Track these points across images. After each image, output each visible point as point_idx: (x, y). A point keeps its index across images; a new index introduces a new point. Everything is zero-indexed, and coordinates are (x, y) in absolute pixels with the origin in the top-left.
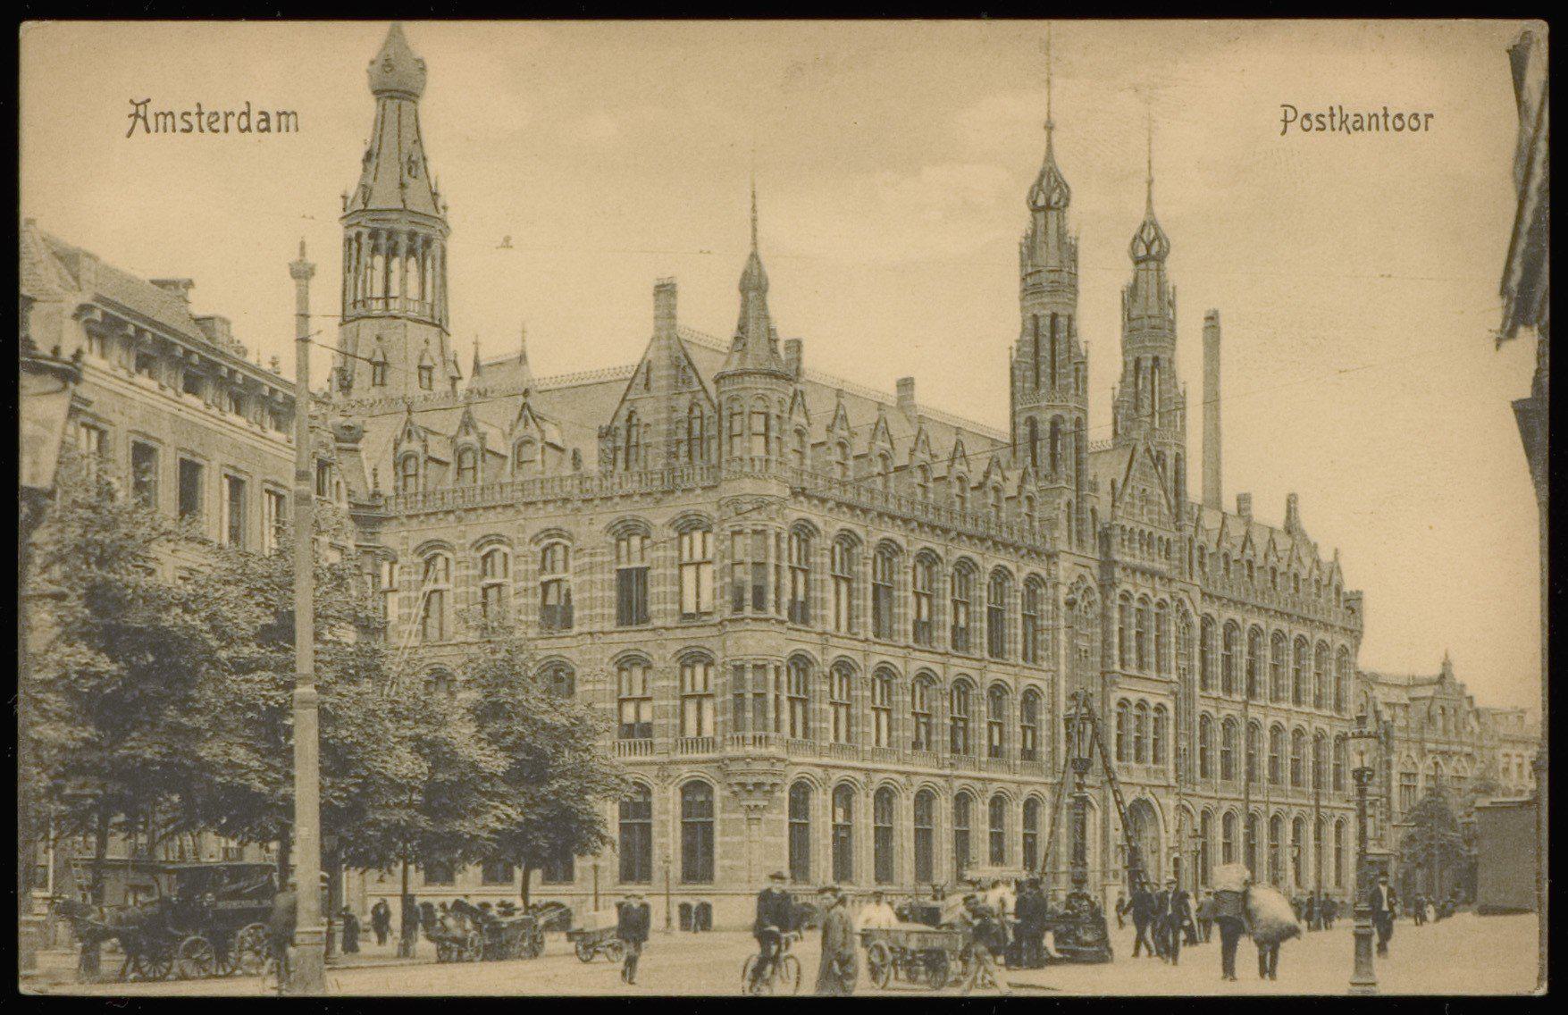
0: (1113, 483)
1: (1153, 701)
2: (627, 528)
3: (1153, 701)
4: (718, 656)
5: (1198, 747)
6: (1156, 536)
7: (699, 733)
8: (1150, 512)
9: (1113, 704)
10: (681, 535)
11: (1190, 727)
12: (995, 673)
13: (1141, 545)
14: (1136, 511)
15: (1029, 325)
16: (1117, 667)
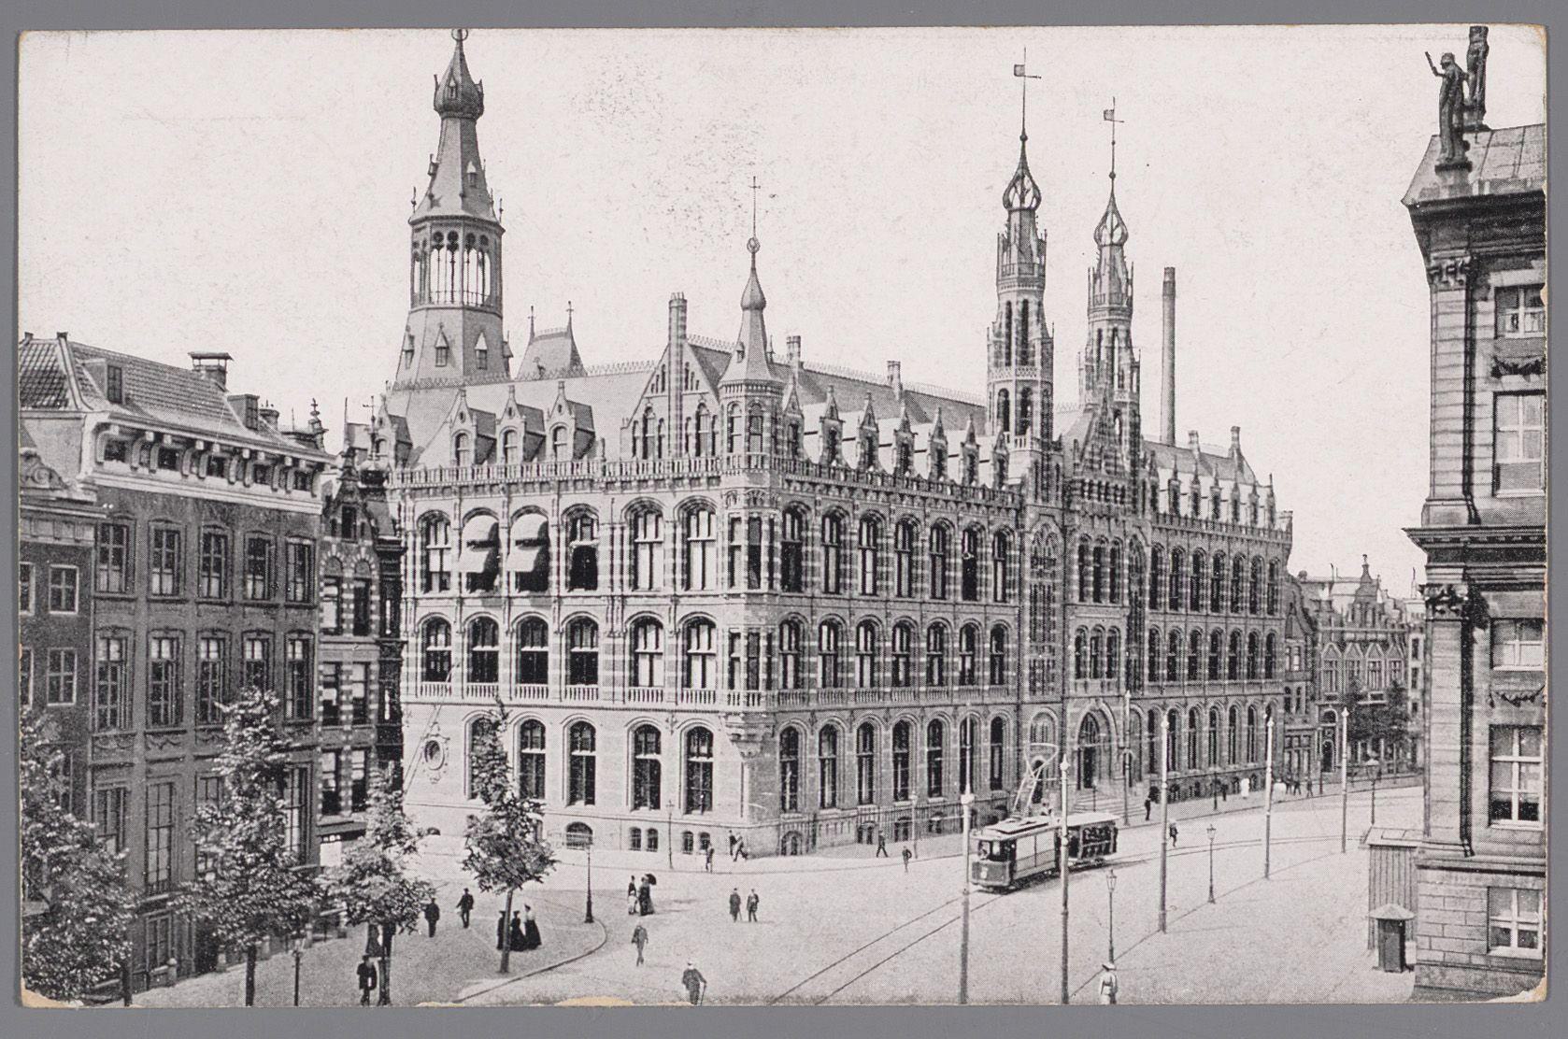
0: (1076, 441)
1: (1108, 626)
2: (644, 507)
3: (1108, 626)
4: (719, 624)
5: (1146, 658)
6: (1112, 485)
7: (704, 685)
8: (1107, 465)
9: (1073, 635)
10: (690, 514)
11: (1139, 639)
12: (969, 613)
13: (1099, 494)
14: (1096, 466)
15: (1004, 309)
16: (1076, 599)
